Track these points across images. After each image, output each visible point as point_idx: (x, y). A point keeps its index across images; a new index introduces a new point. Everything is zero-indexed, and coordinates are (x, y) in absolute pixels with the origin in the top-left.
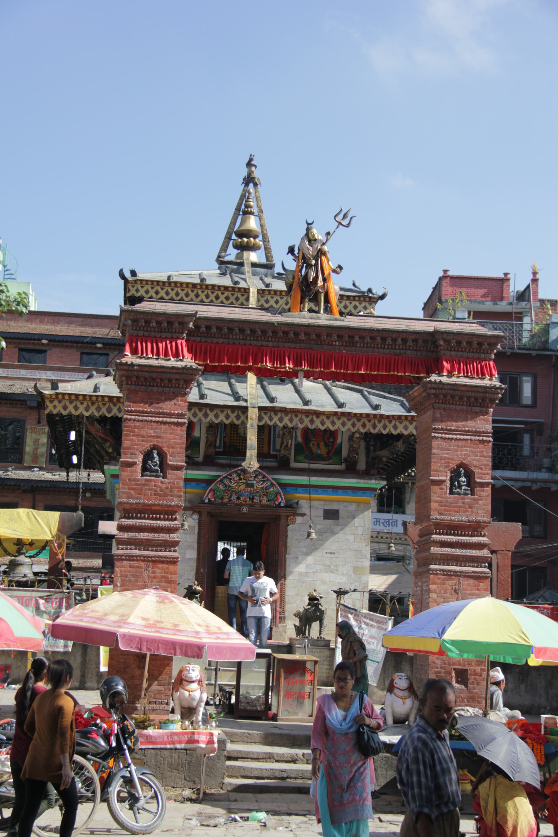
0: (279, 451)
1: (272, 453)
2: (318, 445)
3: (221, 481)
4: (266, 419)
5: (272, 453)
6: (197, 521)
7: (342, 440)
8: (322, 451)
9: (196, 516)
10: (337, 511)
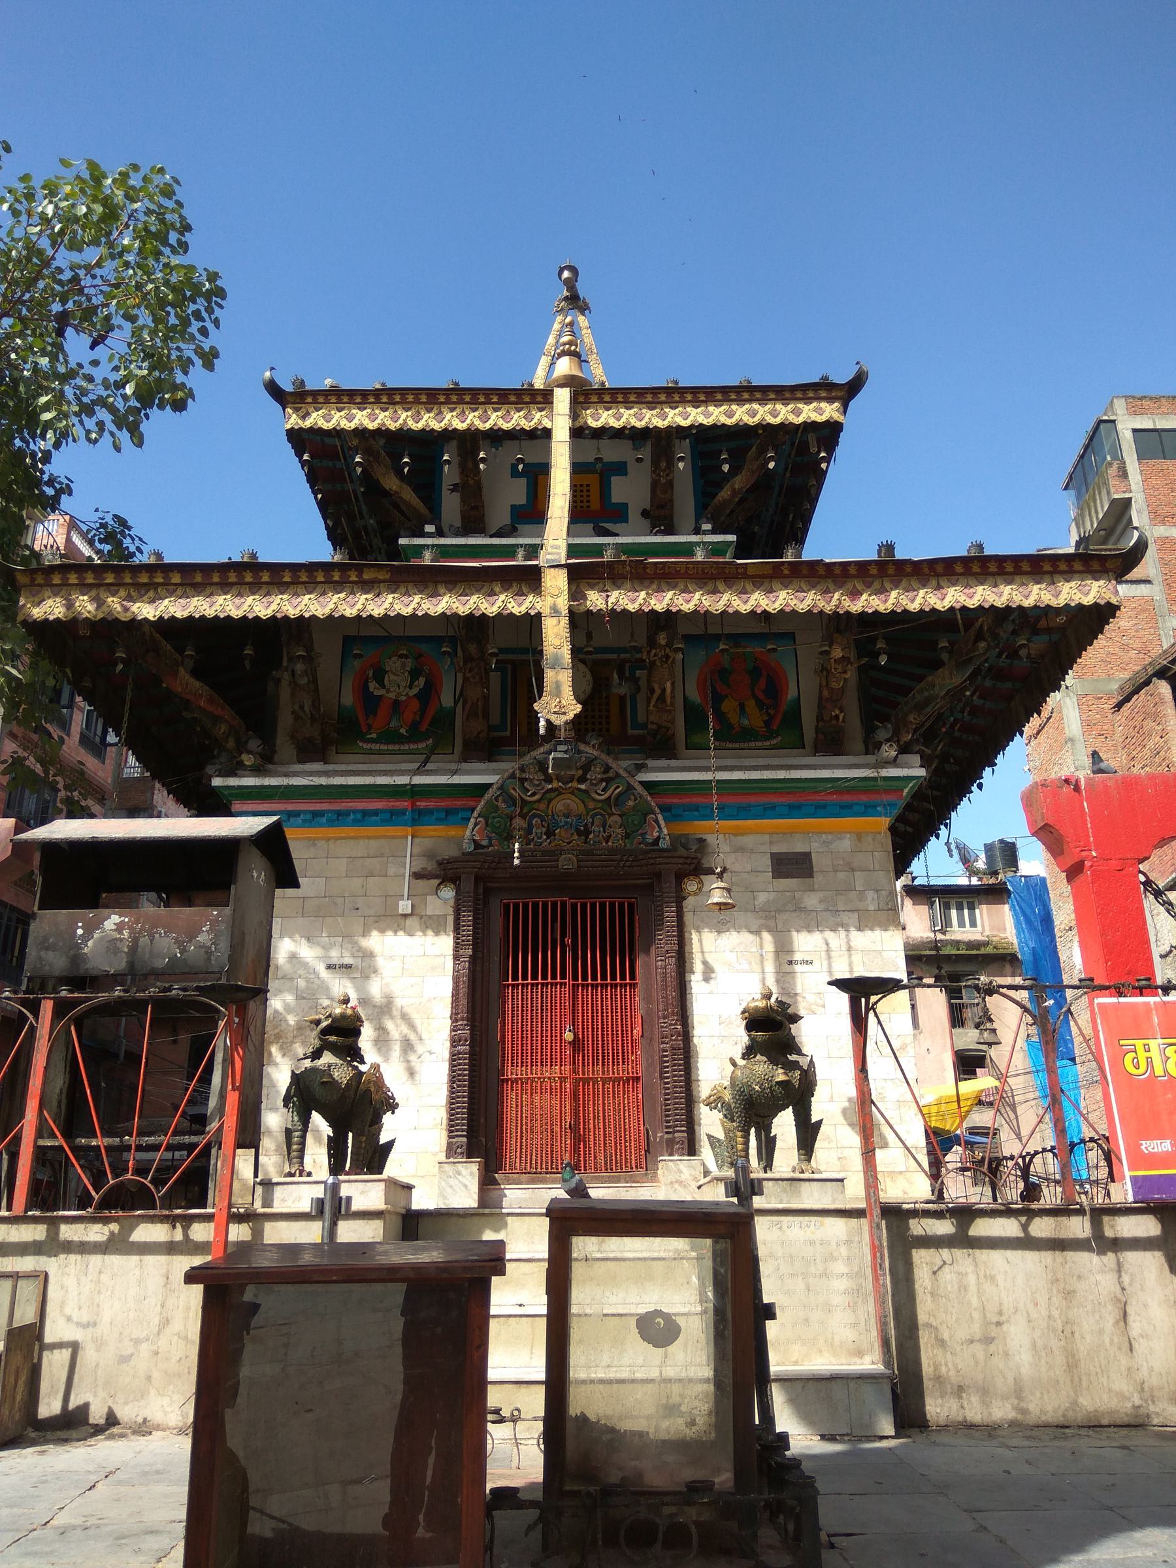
0: (644, 726)
1: (630, 732)
2: (742, 707)
3: (501, 788)
4: (595, 600)
5: (630, 732)
6: (452, 902)
7: (801, 685)
8: (755, 718)
9: (448, 893)
10: (807, 856)
